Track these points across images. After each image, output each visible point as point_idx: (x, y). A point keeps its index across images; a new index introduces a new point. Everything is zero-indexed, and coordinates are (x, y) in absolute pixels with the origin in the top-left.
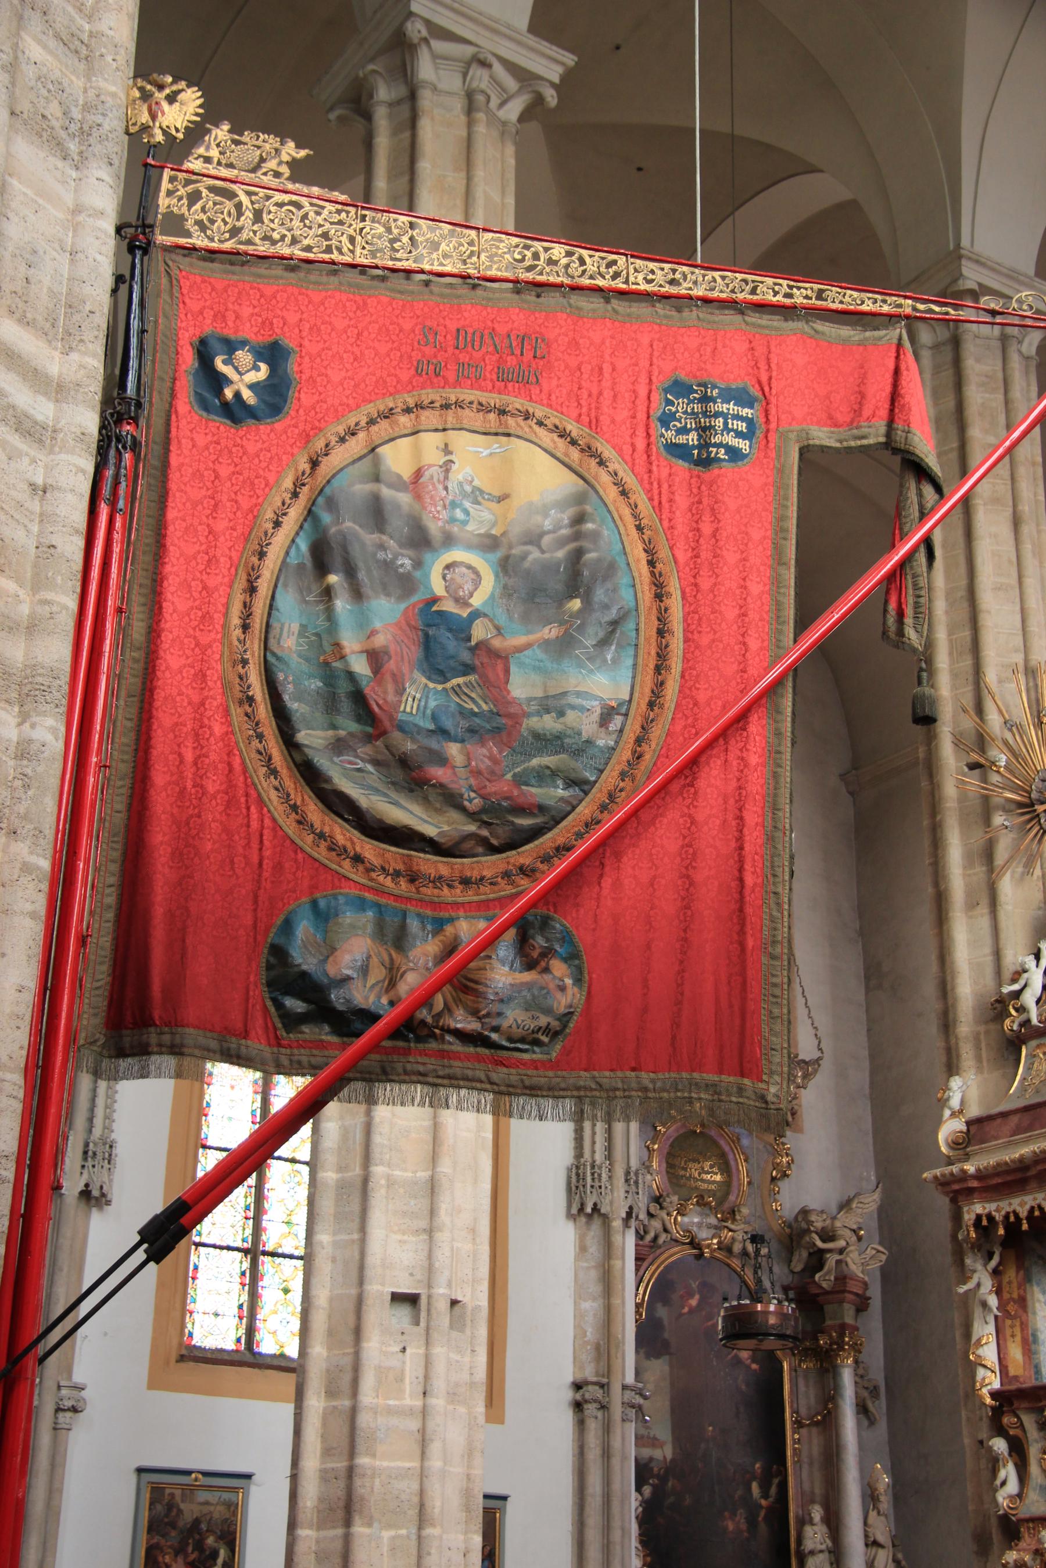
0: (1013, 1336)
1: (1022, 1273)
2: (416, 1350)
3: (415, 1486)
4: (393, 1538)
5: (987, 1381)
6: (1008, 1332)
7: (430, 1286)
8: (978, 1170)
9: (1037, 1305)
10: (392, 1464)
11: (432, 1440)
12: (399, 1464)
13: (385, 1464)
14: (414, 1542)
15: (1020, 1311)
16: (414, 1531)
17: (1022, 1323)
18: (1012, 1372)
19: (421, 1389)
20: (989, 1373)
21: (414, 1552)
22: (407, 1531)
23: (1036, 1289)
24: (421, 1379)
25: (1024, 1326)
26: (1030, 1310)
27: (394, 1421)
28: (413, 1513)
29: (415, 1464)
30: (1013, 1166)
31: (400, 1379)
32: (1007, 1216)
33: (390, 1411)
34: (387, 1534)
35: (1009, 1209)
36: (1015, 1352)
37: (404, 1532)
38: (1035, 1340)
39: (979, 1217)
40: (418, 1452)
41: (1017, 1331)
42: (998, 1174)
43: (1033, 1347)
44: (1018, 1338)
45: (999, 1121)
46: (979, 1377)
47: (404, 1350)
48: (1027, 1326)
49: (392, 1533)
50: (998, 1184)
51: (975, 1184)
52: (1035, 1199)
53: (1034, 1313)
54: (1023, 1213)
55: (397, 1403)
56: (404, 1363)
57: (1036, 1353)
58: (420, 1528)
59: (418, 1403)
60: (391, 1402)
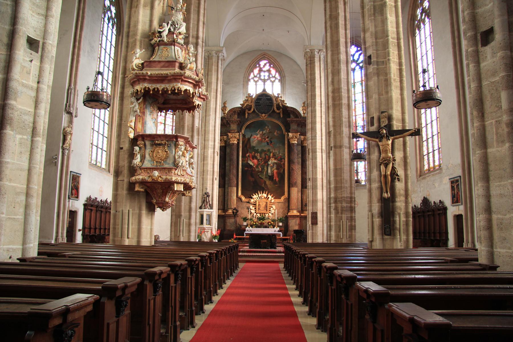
2: (36, 63)
3: (32, 120)
4: (21, 139)
6: (138, 120)
7: (44, 38)
8: (151, 74)
10: (23, 108)
11: (42, 102)
12: (25, 108)
13: (20, 107)
14: (29, 143)
16: (30, 138)
18: (138, 131)
19: (37, 80)
21: (30, 146)
22: (27, 137)
24: (37, 76)
25: (143, 119)
27: (25, 90)
28: (30, 130)
29: (32, 110)
31: (29, 73)
32: (154, 89)
33: (23, 85)
34: (19, 137)
36: (139, 126)
37: (25, 137)
38: (146, 124)
39: (146, 87)
40: (34, 106)
41: (141, 120)
42: (156, 77)
44: (141, 122)
47: (31, 61)
49: (21, 136)
50: (155, 80)
51: (147, 78)
54: (160, 89)
55: (26, 82)
56: (31, 67)
58: (32, 137)
59: (35, 85)
60: (24, 81)
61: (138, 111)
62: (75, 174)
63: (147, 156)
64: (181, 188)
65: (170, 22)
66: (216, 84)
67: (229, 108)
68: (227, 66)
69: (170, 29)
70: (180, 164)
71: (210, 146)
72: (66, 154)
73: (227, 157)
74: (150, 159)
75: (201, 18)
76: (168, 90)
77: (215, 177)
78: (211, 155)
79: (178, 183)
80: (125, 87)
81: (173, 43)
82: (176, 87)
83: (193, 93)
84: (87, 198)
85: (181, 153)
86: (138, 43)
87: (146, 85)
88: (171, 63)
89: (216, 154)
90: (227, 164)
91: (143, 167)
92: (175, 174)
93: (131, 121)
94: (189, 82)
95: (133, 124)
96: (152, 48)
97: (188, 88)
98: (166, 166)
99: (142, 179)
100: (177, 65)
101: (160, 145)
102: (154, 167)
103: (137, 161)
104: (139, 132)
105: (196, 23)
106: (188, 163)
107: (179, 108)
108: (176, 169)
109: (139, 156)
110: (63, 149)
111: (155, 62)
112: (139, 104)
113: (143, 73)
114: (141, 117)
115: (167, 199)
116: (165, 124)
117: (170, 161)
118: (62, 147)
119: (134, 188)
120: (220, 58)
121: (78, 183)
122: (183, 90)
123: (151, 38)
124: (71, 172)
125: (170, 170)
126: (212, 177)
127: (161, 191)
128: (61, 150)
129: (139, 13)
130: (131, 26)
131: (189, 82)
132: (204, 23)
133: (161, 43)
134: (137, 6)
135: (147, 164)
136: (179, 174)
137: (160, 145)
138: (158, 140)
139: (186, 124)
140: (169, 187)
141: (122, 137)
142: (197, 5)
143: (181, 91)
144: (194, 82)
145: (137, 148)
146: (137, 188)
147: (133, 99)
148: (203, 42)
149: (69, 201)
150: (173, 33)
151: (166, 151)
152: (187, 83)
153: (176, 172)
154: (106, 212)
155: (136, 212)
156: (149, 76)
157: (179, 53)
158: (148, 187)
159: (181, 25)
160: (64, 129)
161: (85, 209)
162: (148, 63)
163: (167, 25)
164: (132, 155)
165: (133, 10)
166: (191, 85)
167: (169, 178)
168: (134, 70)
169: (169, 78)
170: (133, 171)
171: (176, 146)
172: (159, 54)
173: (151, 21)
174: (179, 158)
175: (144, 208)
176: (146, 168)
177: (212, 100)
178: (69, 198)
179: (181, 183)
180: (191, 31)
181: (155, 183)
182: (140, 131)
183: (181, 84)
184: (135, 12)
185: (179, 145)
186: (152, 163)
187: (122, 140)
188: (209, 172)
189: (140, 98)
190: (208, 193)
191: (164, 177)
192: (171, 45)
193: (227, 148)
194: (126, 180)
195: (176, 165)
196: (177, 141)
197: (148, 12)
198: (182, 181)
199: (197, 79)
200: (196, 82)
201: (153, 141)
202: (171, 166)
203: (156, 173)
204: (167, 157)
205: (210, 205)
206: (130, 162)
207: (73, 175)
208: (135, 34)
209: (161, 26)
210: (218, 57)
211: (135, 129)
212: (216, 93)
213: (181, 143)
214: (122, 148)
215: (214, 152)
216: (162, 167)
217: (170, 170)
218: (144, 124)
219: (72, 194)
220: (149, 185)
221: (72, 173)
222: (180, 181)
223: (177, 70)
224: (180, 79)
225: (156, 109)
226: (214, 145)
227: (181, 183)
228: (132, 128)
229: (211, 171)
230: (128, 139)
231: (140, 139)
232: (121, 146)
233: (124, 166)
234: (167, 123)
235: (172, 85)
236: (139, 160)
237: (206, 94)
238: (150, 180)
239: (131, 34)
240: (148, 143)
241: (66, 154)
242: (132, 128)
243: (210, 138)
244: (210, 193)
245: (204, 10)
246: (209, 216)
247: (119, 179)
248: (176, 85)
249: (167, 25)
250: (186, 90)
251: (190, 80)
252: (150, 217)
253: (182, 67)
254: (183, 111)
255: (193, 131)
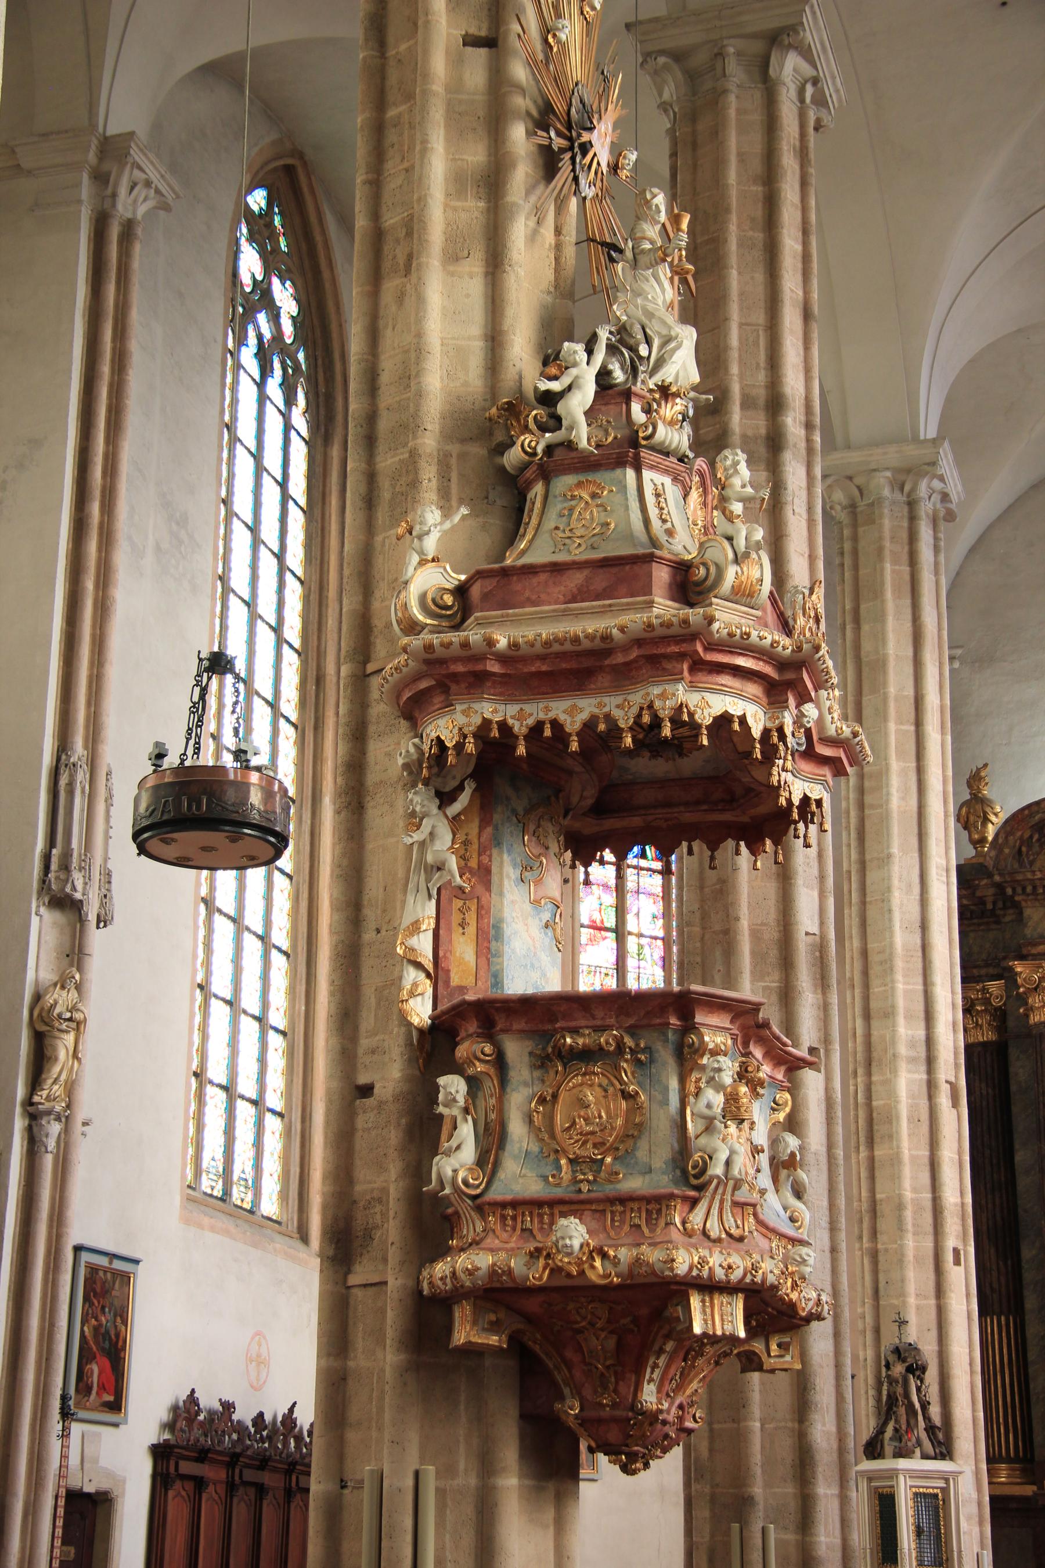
0: (463, 925)
1: (489, 830)
5: (419, 991)
6: (456, 918)
8: (514, 645)
9: (506, 882)
15: (480, 890)
17: (480, 908)
18: (455, 980)
20: (422, 976)
23: (505, 856)
25: (482, 912)
26: (494, 888)
30: (586, 644)
32: (537, 728)
35: (542, 716)
38: (499, 936)
39: (486, 723)
41: (471, 917)
42: (542, 658)
43: (493, 945)
44: (471, 929)
45: (543, 577)
46: (407, 984)
48: (488, 912)
50: (539, 674)
51: (494, 667)
52: (600, 705)
53: (501, 894)
54: (572, 724)
57: (499, 954)
61: (453, 862)
62: (103, 1261)
63: (517, 1128)
64: (729, 1318)
65: (604, 334)
66: (909, 669)
67: (1005, 802)
68: (972, 550)
69: (603, 375)
70: (717, 1169)
71: (903, 1050)
72: (51, 1144)
73: (1015, 1109)
74: (535, 1148)
75: (791, 284)
76: (615, 730)
77: (951, 1242)
78: (913, 1108)
79: (710, 1287)
80: (372, 729)
81: (629, 450)
82: (665, 709)
83: (766, 733)
84: (175, 1409)
85: (718, 1100)
86: (429, 475)
87: (491, 709)
88: (622, 571)
89: (944, 1100)
90: (1018, 1158)
91: (496, 1193)
92: (688, 1233)
93: (415, 928)
94: (737, 671)
95: (423, 944)
96: (508, 498)
97: (736, 707)
98: (633, 1184)
99: (493, 1272)
100: (661, 575)
101: (587, 1055)
102: (558, 1193)
103: (458, 1160)
104: (462, 989)
105: (759, 317)
106: (764, 1159)
107: (690, 832)
108: (694, 1203)
109: (466, 1131)
110: (34, 1116)
111: (530, 570)
112: (455, 822)
113: (465, 645)
114: (468, 900)
115: (649, 1396)
116: (620, 932)
117: (657, 1149)
118: (29, 1102)
119: (448, 1330)
120: (926, 508)
121: (122, 1314)
122: (705, 717)
123: (500, 437)
124: (78, 1249)
125: (655, 1205)
126: (929, 1244)
127: (611, 1343)
128: (19, 1124)
129: (421, 300)
130: (385, 378)
131: (737, 671)
132: (807, 316)
133: (562, 460)
134: (410, 265)
135: (519, 1177)
136: (714, 1228)
137: (587, 1055)
138: (575, 1031)
139: (744, 924)
140: (658, 1314)
141: (367, 1020)
142: (759, 212)
143: (695, 727)
144: (768, 670)
145: (453, 1086)
146: (464, 1332)
147: (421, 799)
148: (809, 426)
149: (65, 1434)
150: (627, 395)
151: (626, 1096)
152: (726, 680)
153: (697, 1218)
154: (289, 1493)
155: (459, 1481)
156: (502, 658)
157: (665, 507)
158: (529, 1319)
159: (667, 340)
160: (37, 997)
161: (161, 1481)
162: (489, 584)
163: (590, 352)
164: (425, 1130)
165: (390, 286)
166: (753, 689)
167: (653, 1256)
168: (412, 627)
169: (620, 658)
170: (434, 1223)
171: (688, 1056)
172: (550, 522)
173: (495, 340)
174: (709, 1128)
175: (509, 1454)
176: (515, 1204)
177: (895, 765)
178: (66, 1414)
179: (727, 1289)
180: (734, 369)
181: (568, 1292)
182: (470, 981)
183: (693, 686)
184: (401, 298)
185: (701, 1050)
186: (549, 1171)
187: (365, 1043)
188: (908, 1214)
189: (461, 788)
190: (912, 1348)
191: (624, 1254)
192: (620, 462)
193: (1013, 1053)
194: (396, 1283)
195: (692, 1178)
196: (689, 1027)
197: (474, 287)
198: (736, 1276)
199: (785, 645)
200: (782, 665)
201: (545, 1036)
202: (662, 1182)
203: (575, 1233)
204: (635, 1130)
205: (931, 1429)
206: (418, 1170)
207: (93, 1270)
208: (410, 426)
209: (551, 360)
210: (912, 504)
211: (437, 974)
212: (919, 723)
213: (712, 1039)
214: (366, 1091)
215: (931, 1085)
216: (609, 1190)
217: (655, 1205)
218: (489, 940)
219: (84, 1387)
220: (532, 1305)
221: (85, 1257)
222: (720, 1274)
223: (663, 608)
224: (681, 656)
225: (554, 847)
226: (930, 1041)
227: (727, 1289)
228: (419, 966)
229: (918, 1209)
230: (398, 1032)
231: (472, 1027)
232: (363, 1079)
233: (381, 1199)
234: (631, 925)
235: (637, 698)
236: (468, 1154)
237: (847, 731)
238: (537, 1274)
239: (384, 424)
240: (515, 1050)
241: (51, 1144)
242: (419, 966)
243: (901, 1003)
244: (929, 1350)
245: (805, 232)
246: (935, 1507)
247: (353, 1280)
248: (663, 696)
249: (590, 352)
250: (724, 719)
251: (741, 662)
252: (550, 1514)
253: (690, 585)
254: (713, 846)
255: (787, 963)
